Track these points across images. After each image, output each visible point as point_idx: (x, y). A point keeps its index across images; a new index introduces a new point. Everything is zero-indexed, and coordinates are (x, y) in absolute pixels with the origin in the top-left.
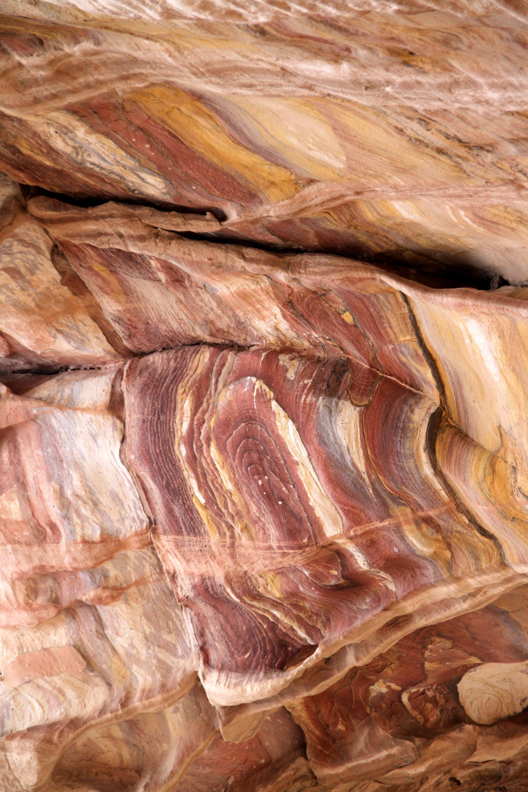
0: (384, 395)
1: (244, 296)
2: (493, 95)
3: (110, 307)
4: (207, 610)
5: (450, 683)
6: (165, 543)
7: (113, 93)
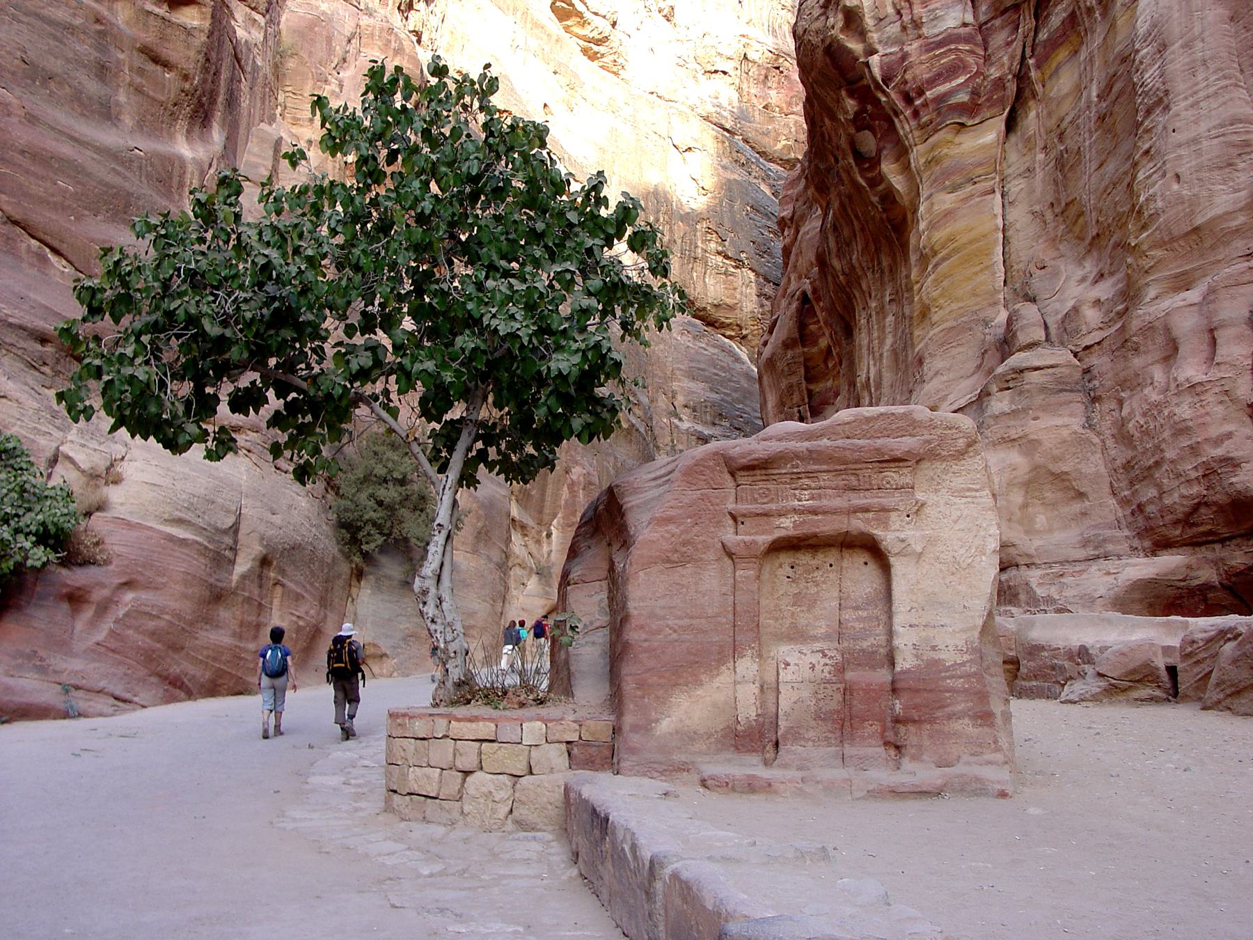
0: (971, 109)
2: (1087, 143)
3: (997, 22)
4: (899, 55)
6: (920, 42)
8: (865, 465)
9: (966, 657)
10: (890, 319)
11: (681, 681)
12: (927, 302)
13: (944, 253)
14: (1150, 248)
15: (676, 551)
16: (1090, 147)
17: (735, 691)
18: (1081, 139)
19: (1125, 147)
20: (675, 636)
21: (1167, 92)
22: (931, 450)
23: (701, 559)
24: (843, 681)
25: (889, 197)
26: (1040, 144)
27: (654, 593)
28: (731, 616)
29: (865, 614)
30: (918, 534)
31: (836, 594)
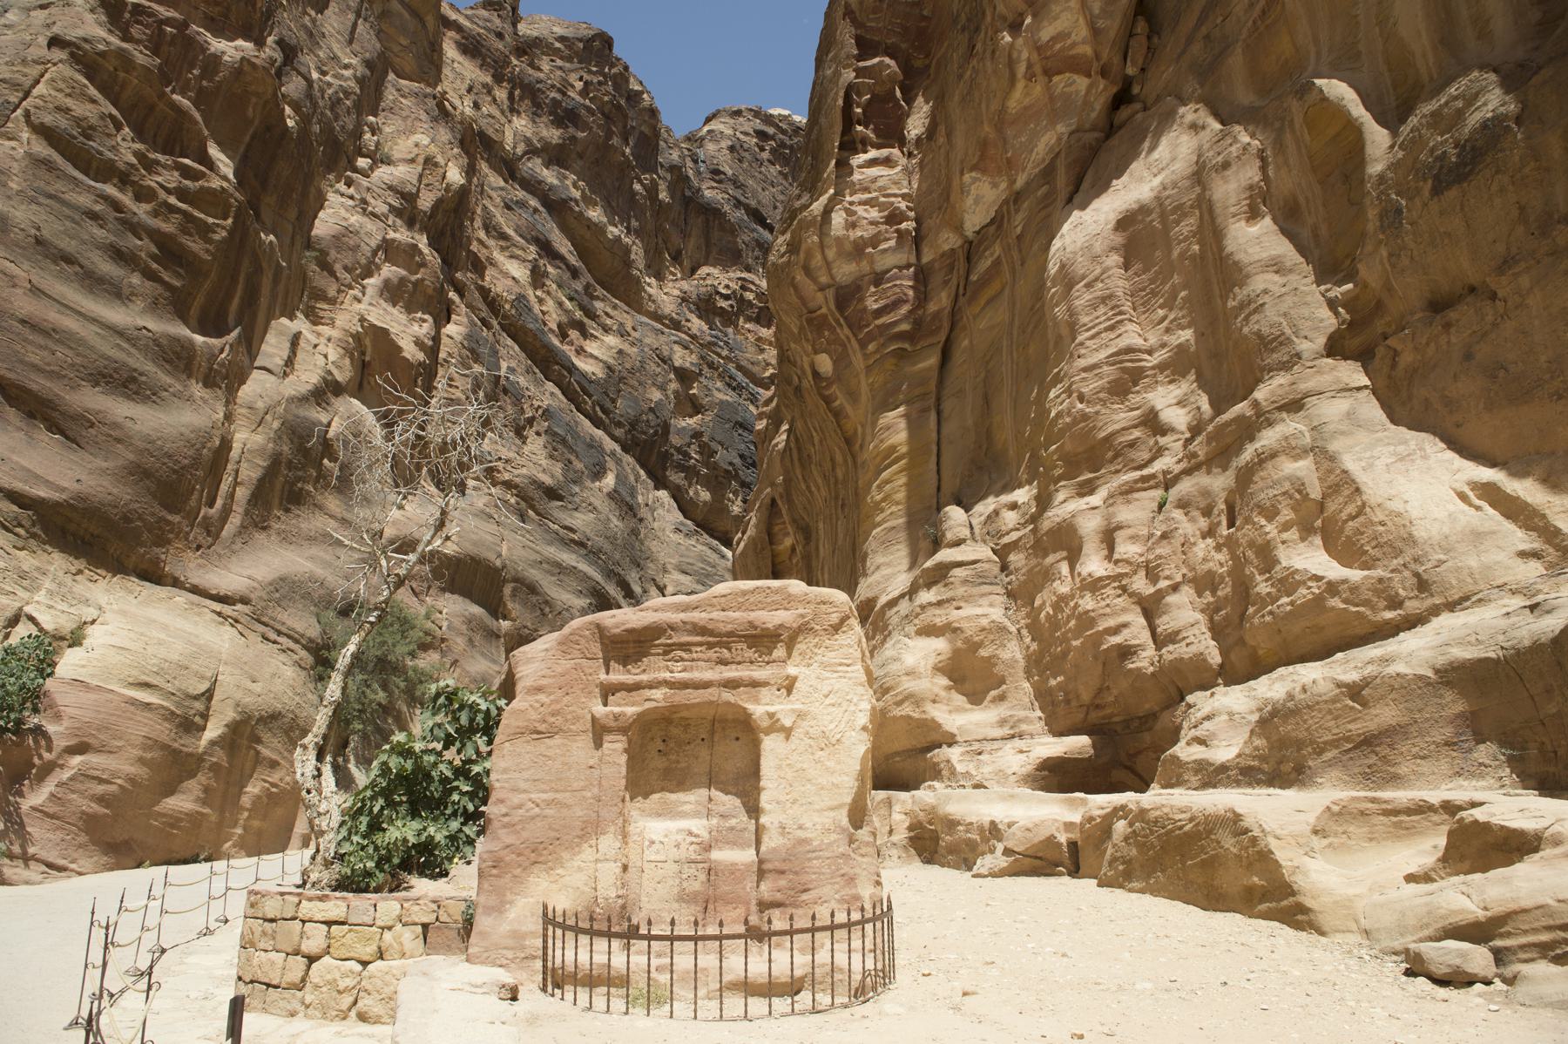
9: (834, 837)
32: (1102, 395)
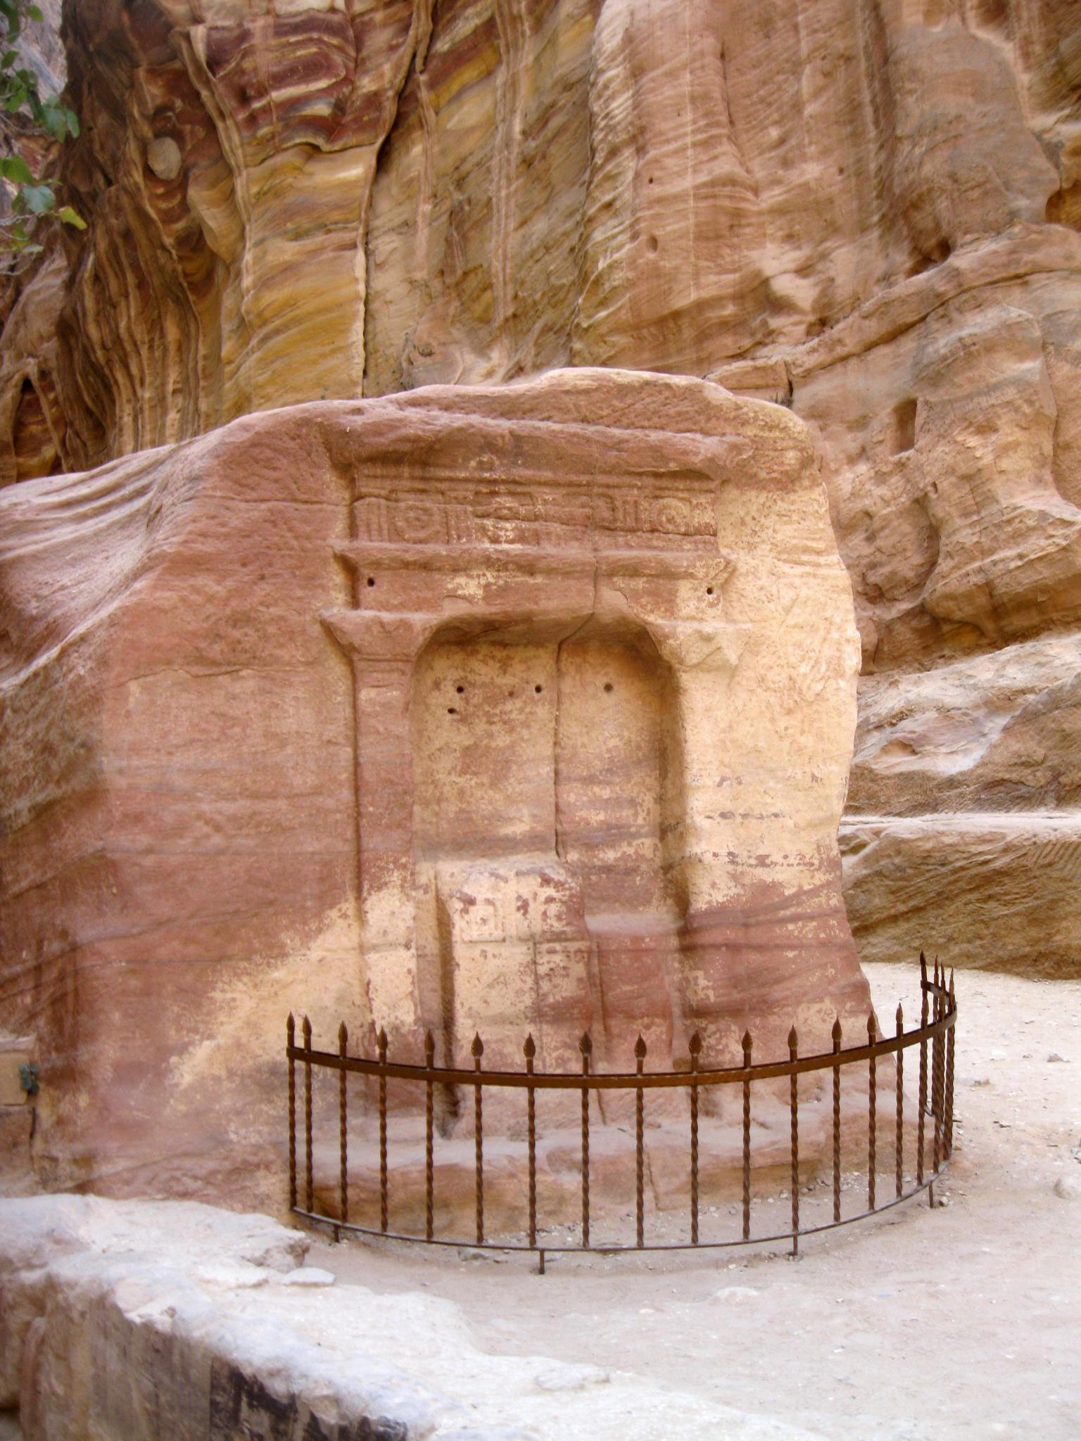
0: (331, 127)
1: (382, 76)
2: (503, 193)
3: (379, 16)
4: (236, 33)
5: (178, 137)
6: (270, 20)
7: (498, 37)
8: (627, 480)
9: (820, 878)
10: (173, 416)
11: (236, 948)
12: (249, 389)
13: (277, 323)
14: (611, 332)
15: (218, 636)
16: (508, 197)
17: (363, 968)
18: (493, 187)
19: (566, 200)
20: (217, 840)
21: (642, 130)
22: (742, 465)
23: (277, 660)
24: (584, 934)
25: (194, 240)
26: (426, 190)
27: (165, 735)
28: (346, 794)
29: (606, 793)
30: (730, 628)
31: (548, 750)
32: (683, 243)
